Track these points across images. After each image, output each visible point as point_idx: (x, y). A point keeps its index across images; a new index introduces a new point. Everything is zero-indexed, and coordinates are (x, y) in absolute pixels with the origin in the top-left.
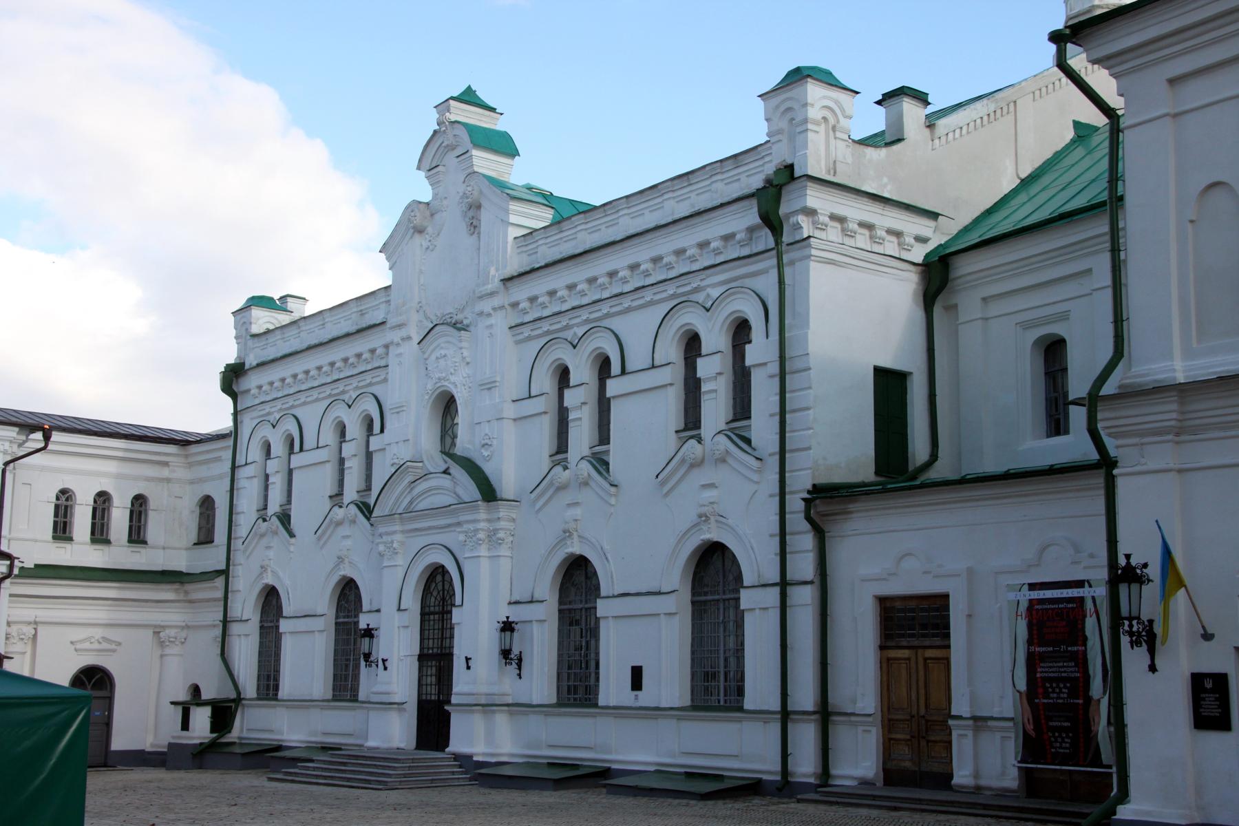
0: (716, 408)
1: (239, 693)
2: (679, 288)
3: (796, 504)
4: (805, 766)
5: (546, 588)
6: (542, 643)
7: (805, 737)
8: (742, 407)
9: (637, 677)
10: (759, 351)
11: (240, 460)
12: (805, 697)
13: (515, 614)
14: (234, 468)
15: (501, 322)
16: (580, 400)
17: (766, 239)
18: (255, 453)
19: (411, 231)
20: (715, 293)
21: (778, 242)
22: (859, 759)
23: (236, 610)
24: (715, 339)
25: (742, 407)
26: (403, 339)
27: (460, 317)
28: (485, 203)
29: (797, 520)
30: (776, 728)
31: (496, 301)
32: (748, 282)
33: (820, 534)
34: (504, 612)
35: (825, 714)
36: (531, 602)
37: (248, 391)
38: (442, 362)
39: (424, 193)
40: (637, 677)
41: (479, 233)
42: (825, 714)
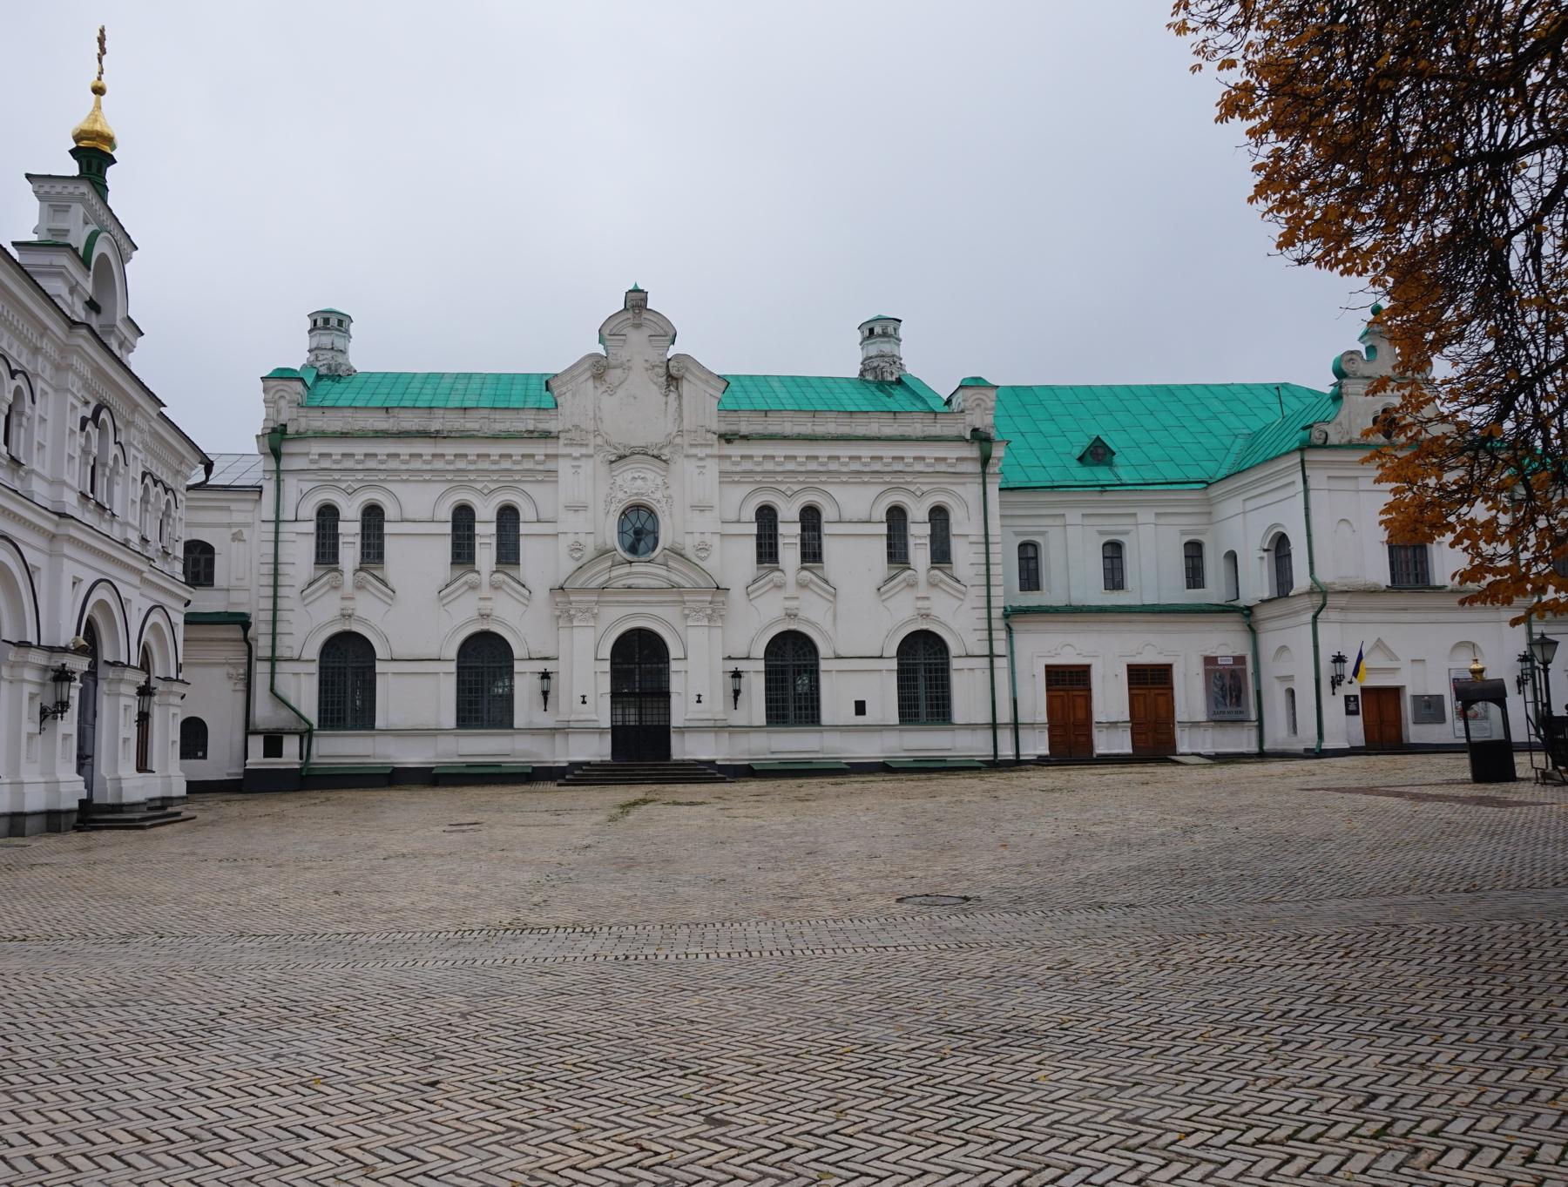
0: (920, 554)
1: (311, 725)
2: (896, 476)
3: (997, 613)
4: (1006, 752)
5: (760, 651)
6: (755, 685)
7: (1005, 738)
8: (941, 554)
9: (860, 708)
10: (964, 524)
11: (288, 514)
12: (1004, 716)
13: (741, 666)
14: (277, 522)
15: (713, 467)
16: (789, 533)
17: (977, 468)
18: (309, 510)
19: (588, 374)
20: (925, 488)
21: (984, 473)
22: (1037, 744)
23: (286, 647)
24: (918, 513)
25: (941, 554)
26: (582, 455)
27: (655, 452)
28: (688, 375)
29: (998, 624)
30: (990, 733)
31: (708, 451)
32: (954, 488)
33: (1009, 631)
34: (732, 666)
35: (1016, 726)
36: (748, 658)
37: (307, 454)
38: (639, 482)
39: (601, 350)
40: (860, 708)
41: (680, 396)
42: (1016, 726)
